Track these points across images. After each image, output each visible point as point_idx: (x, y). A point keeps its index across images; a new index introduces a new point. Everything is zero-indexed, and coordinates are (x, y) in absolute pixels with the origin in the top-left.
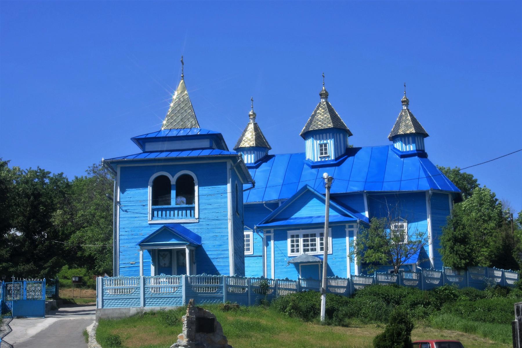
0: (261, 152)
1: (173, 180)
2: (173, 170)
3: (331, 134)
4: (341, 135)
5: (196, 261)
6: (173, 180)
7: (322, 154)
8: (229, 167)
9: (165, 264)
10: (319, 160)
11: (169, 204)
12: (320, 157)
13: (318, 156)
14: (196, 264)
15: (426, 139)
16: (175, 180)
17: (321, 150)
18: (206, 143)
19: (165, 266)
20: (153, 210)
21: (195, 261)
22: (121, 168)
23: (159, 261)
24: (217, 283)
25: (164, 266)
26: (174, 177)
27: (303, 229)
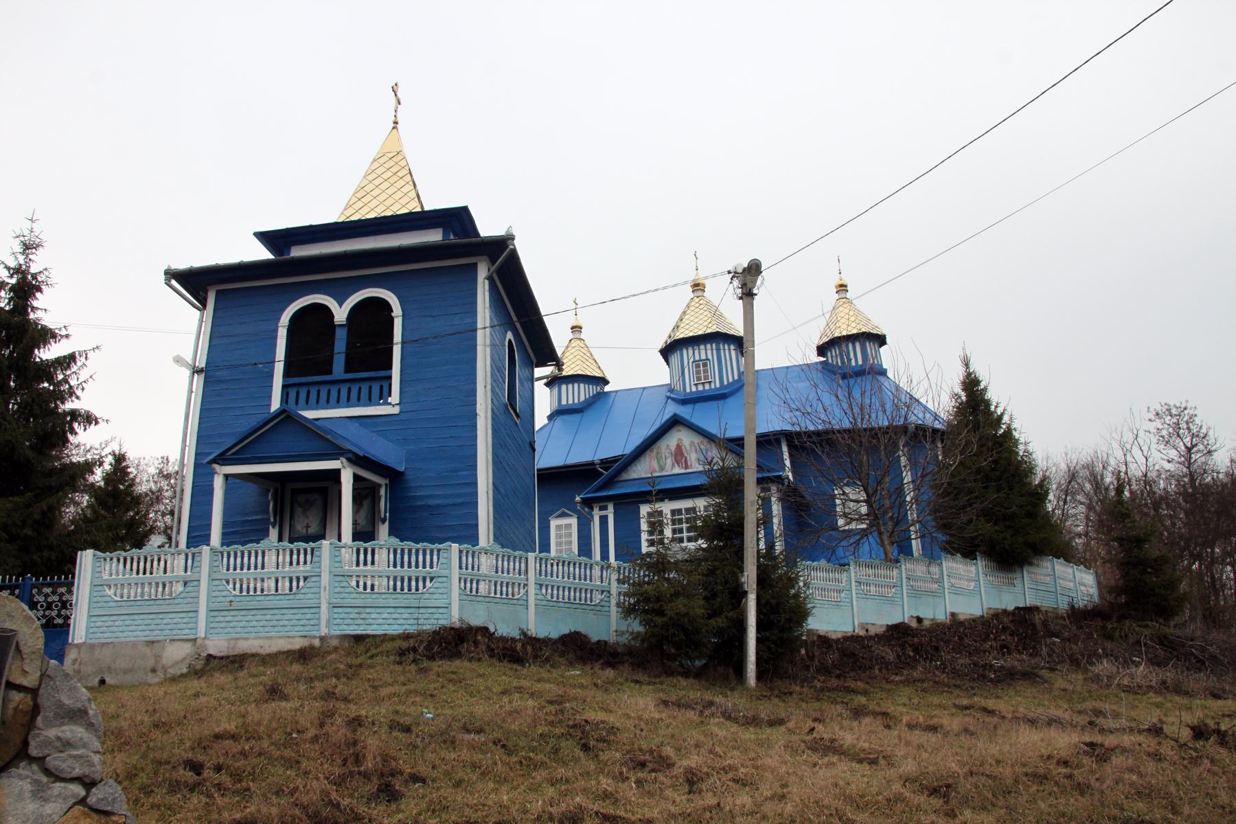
0: (591, 386)
1: (341, 314)
2: (340, 291)
3: (714, 345)
4: (732, 347)
5: (388, 515)
6: (341, 314)
7: (699, 379)
8: (482, 272)
9: (308, 527)
10: (694, 389)
11: (330, 372)
12: (696, 385)
13: (692, 383)
14: (387, 523)
15: (883, 349)
16: (346, 315)
17: (698, 372)
18: (434, 236)
19: (307, 530)
20: (284, 387)
21: (385, 516)
22: (218, 293)
23: (292, 518)
24: (431, 567)
25: (304, 531)
26: (344, 306)
27: (671, 499)
